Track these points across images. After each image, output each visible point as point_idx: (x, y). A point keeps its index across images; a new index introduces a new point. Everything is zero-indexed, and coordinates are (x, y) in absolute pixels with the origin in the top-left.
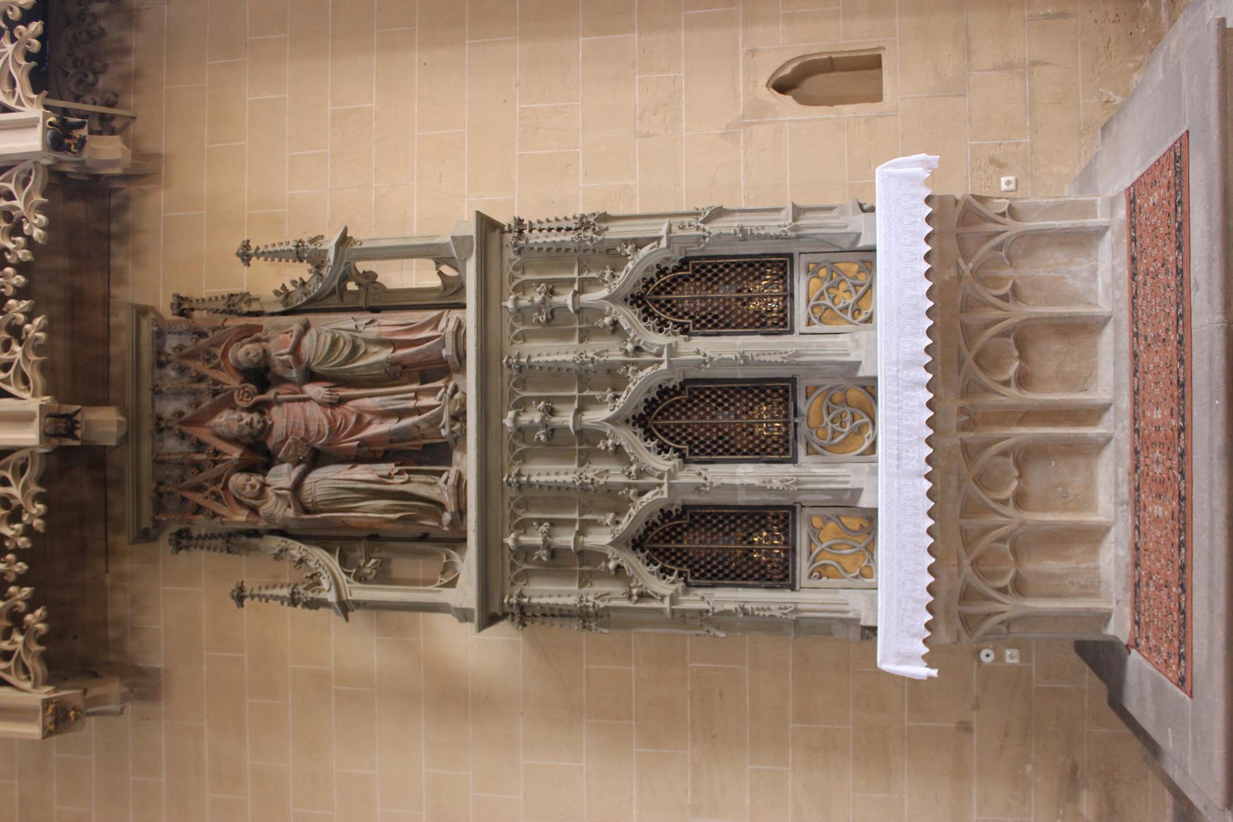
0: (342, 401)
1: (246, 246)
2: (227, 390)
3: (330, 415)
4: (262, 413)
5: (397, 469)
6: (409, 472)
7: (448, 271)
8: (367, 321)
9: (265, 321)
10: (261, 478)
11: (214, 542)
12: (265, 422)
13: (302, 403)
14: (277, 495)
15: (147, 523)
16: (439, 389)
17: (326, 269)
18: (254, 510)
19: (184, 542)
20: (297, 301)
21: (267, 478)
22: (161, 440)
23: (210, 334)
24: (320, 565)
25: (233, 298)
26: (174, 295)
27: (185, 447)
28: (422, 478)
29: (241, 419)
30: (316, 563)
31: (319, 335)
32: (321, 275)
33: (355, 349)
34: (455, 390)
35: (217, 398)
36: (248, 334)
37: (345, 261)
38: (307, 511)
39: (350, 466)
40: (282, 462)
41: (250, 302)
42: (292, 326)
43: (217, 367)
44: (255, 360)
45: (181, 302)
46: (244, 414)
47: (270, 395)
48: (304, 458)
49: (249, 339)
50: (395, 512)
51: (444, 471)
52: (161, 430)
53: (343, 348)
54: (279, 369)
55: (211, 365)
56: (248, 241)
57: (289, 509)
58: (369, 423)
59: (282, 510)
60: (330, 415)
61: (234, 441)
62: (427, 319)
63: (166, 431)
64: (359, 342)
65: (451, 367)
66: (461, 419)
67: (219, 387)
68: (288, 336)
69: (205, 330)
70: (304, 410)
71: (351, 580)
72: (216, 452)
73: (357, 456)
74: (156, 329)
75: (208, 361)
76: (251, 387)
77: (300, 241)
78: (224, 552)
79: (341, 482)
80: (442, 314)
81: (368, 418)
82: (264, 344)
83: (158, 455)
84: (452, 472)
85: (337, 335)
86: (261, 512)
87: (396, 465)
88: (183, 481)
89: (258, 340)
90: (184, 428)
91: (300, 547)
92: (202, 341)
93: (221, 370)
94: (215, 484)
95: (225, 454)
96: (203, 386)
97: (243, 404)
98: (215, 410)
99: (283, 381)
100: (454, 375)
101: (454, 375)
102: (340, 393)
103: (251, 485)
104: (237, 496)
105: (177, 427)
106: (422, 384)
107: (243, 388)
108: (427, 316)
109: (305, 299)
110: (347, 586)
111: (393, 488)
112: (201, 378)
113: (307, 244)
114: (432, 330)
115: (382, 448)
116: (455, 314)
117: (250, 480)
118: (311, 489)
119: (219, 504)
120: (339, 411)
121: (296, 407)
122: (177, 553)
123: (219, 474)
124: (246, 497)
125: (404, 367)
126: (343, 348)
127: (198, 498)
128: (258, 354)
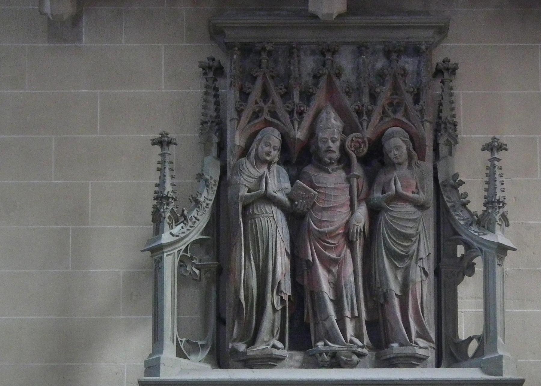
0: (351, 244)
1: (501, 147)
2: (362, 125)
3: (337, 232)
4: (339, 161)
5: (286, 298)
6: (283, 310)
7: (473, 346)
8: (426, 268)
9: (428, 165)
10: (277, 159)
11: (212, 107)
12: (331, 164)
13: (349, 203)
14: (261, 177)
15: (231, 36)
16: (362, 341)
17: (477, 230)
18: (245, 152)
19: (211, 75)
20: (447, 197)
21: (276, 165)
22: (313, 53)
23: (417, 107)
24: (195, 222)
25: (452, 127)
26: (457, 64)
27: (307, 79)
28: (278, 323)
29: (333, 142)
30: (196, 218)
31: (414, 220)
32: (471, 225)
33: (401, 258)
34: (360, 355)
35: (355, 115)
36: (417, 145)
37: (484, 249)
38: (245, 208)
39: (289, 251)
40: (292, 183)
41: (447, 145)
42: (423, 191)
43: (384, 114)
44: (391, 155)
45: (450, 71)
46: (338, 143)
47: (357, 170)
48: (297, 205)
49: (411, 149)
50: (246, 297)
51: (284, 343)
52: (323, 54)
53: (402, 246)
54: (382, 178)
55: (386, 109)
56: (506, 150)
57: (247, 189)
58: (329, 271)
59: (246, 183)
60: (337, 232)
61: (312, 133)
62: (427, 327)
63: (322, 58)
64: (407, 261)
65: (383, 351)
66: (334, 361)
67: (365, 117)
68: (414, 189)
69: (421, 102)
70: (342, 205)
71: (181, 253)
72: (301, 114)
73: (298, 257)
74: (423, 47)
75: (391, 104)
76: (365, 150)
77: (504, 204)
78: (202, 118)
79: (274, 243)
80: (432, 342)
81: (335, 270)
82: (407, 164)
83: (298, 50)
84: (285, 353)
85: (414, 239)
86: (243, 159)
87: (289, 296)
88: (273, 77)
89: (410, 157)
90: (324, 78)
91: (210, 200)
92: (409, 99)
93: (382, 119)
94: (269, 111)
95: (299, 123)
96: (366, 99)
97: (348, 143)
98: (341, 112)
99: (371, 181)
100: (374, 353)
101: (374, 353)
102: (358, 242)
103: (270, 152)
104: (258, 137)
105: (325, 71)
106: (366, 321)
107: (364, 142)
108: (430, 327)
109: (449, 205)
110: (176, 251)
111: (269, 295)
112: (373, 97)
113: (501, 211)
114: (417, 332)
115: (306, 283)
116: (432, 355)
117: (275, 150)
118: (267, 213)
119: (250, 115)
120: (340, 241)
121: (345, 198)
122: (200, 67)
123: (280, 115)
124: (258, 146)
125: (382, 305)
126: (402, 246)
127: (256, 93)
128: (397, 158)
